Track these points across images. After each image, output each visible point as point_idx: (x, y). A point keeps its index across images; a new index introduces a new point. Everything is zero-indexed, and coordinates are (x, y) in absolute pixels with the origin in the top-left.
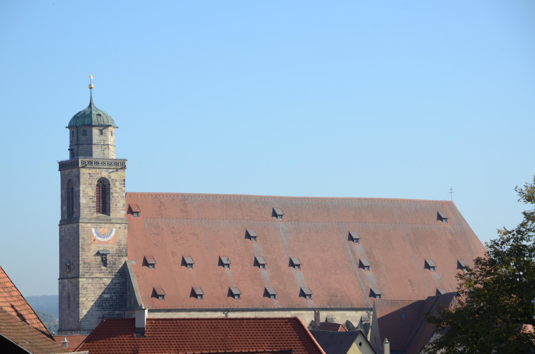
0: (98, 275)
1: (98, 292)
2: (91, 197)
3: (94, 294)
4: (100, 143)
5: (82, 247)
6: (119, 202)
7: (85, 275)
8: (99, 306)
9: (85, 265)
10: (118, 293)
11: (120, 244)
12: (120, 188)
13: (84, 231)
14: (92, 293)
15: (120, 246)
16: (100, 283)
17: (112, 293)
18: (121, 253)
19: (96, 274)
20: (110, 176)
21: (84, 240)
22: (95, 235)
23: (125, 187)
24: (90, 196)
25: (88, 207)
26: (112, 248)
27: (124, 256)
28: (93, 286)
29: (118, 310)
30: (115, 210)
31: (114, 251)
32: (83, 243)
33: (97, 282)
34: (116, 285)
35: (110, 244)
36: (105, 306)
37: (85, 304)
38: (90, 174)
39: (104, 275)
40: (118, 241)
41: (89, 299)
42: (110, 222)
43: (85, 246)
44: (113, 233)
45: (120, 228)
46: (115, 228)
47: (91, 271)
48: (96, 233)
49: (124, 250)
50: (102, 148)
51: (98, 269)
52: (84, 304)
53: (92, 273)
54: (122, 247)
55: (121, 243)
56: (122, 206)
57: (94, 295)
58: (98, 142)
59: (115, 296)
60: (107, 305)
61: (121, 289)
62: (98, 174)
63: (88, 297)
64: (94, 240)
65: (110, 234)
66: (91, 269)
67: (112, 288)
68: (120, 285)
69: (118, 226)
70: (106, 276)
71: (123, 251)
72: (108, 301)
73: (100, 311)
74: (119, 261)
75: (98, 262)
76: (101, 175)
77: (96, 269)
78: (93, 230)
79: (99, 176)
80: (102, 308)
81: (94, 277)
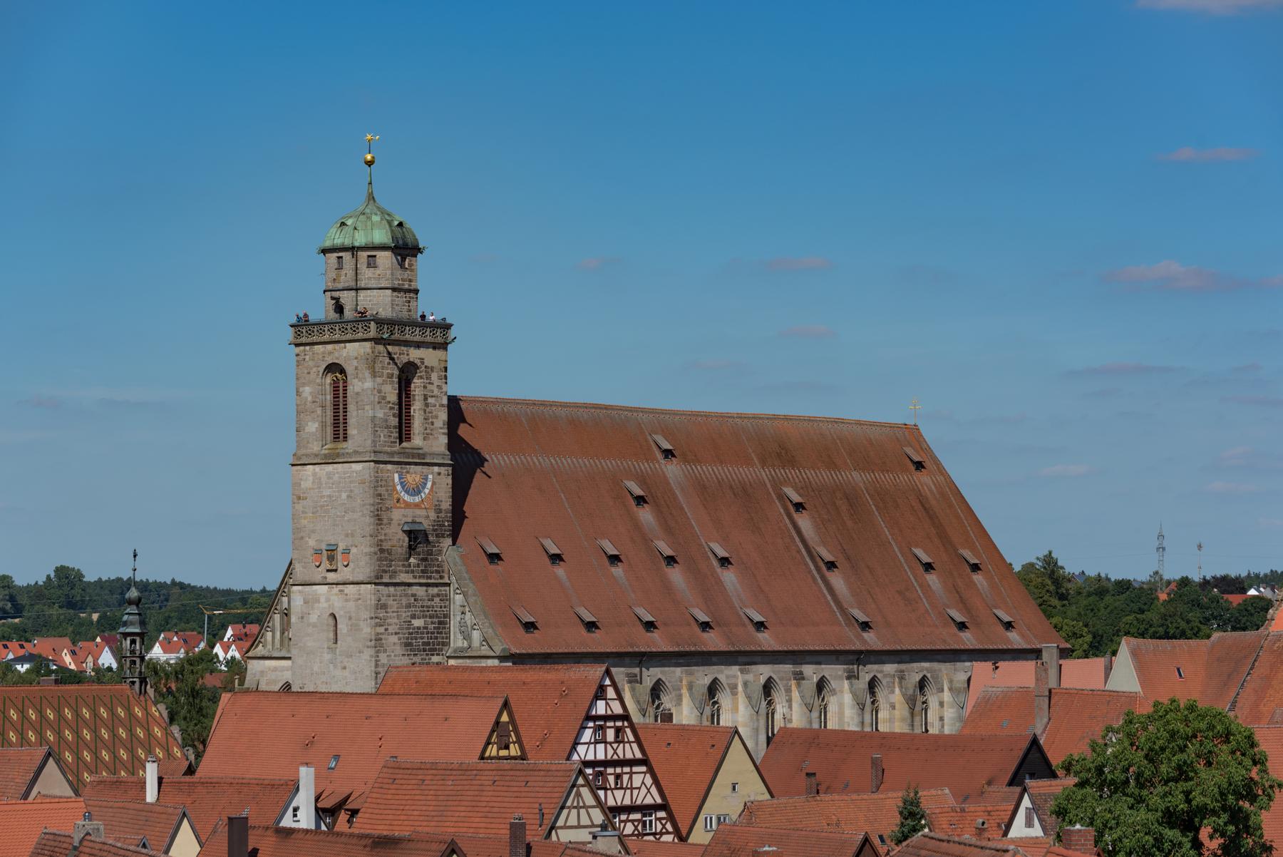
1: (404, 615)
2: (391, 405)
3: (398, 619)
5: (378, 515)
6: (436, 417)
7: (382, 576)
8: (407, 645)
9: (382, 555)
10: (437, 617)
13: (381, 480)
14: (394, 617)
15: (440, 515)
16: (406, 595)
17: (426, 616)
18: (442, 531)
19: (401, 574)
20: (423, 359)
22: (399, 488)
23: (446, 383)
24: (389, 402)
25: (388, 427)
29: (438, 655)
30: (431, 434)
32: (380, 506)
34: (433, 600)
36: (415, 646)
37: (384, 641)
40: (437, 503)
41: (390, 631)
42: (421, 460)
44: (429, 485)
45: (439, 474)
46: (432, 473)
47: (393, 568)
48: (401, 483)
49: (446, 524)
50: (406, 297)
52: (381, 639)
53: (395, 572)
54: (443, 515)
55: (441, 507)
56: (442, 426)
57: (396, 621)
59: (432, 623)
60: (419, 642)
61: (441, 607)
62: (403, 354)
63: (388, 625)
64: (398, 501)
65: (424, 488)
66: (393, 563)
67: (428, 607)
68: (441, 600)
69: (436, 469)
70: (417, 581)
71: (444, 526)
72: (421, 633)
73: (408, 655)
74: (438, 546)
75: (404, 549)
76: (407, 357)
78: (396, 476)
79: (404, 359)
80: (411, 650)
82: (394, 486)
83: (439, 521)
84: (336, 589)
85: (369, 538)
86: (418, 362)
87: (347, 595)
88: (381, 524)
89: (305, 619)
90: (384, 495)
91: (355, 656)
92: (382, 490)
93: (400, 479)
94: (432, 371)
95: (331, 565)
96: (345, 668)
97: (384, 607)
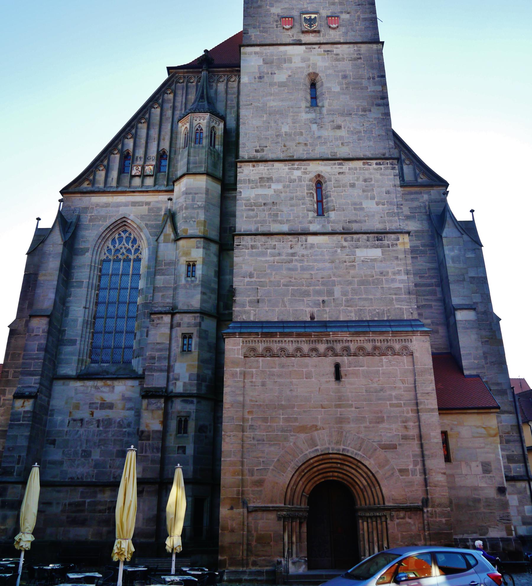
84: (317, 49)
85: (367, 6)
87: (337, 55)
89: (266, 79)
91: (356, 114)
95: (311, 27)
96: (339, 127)
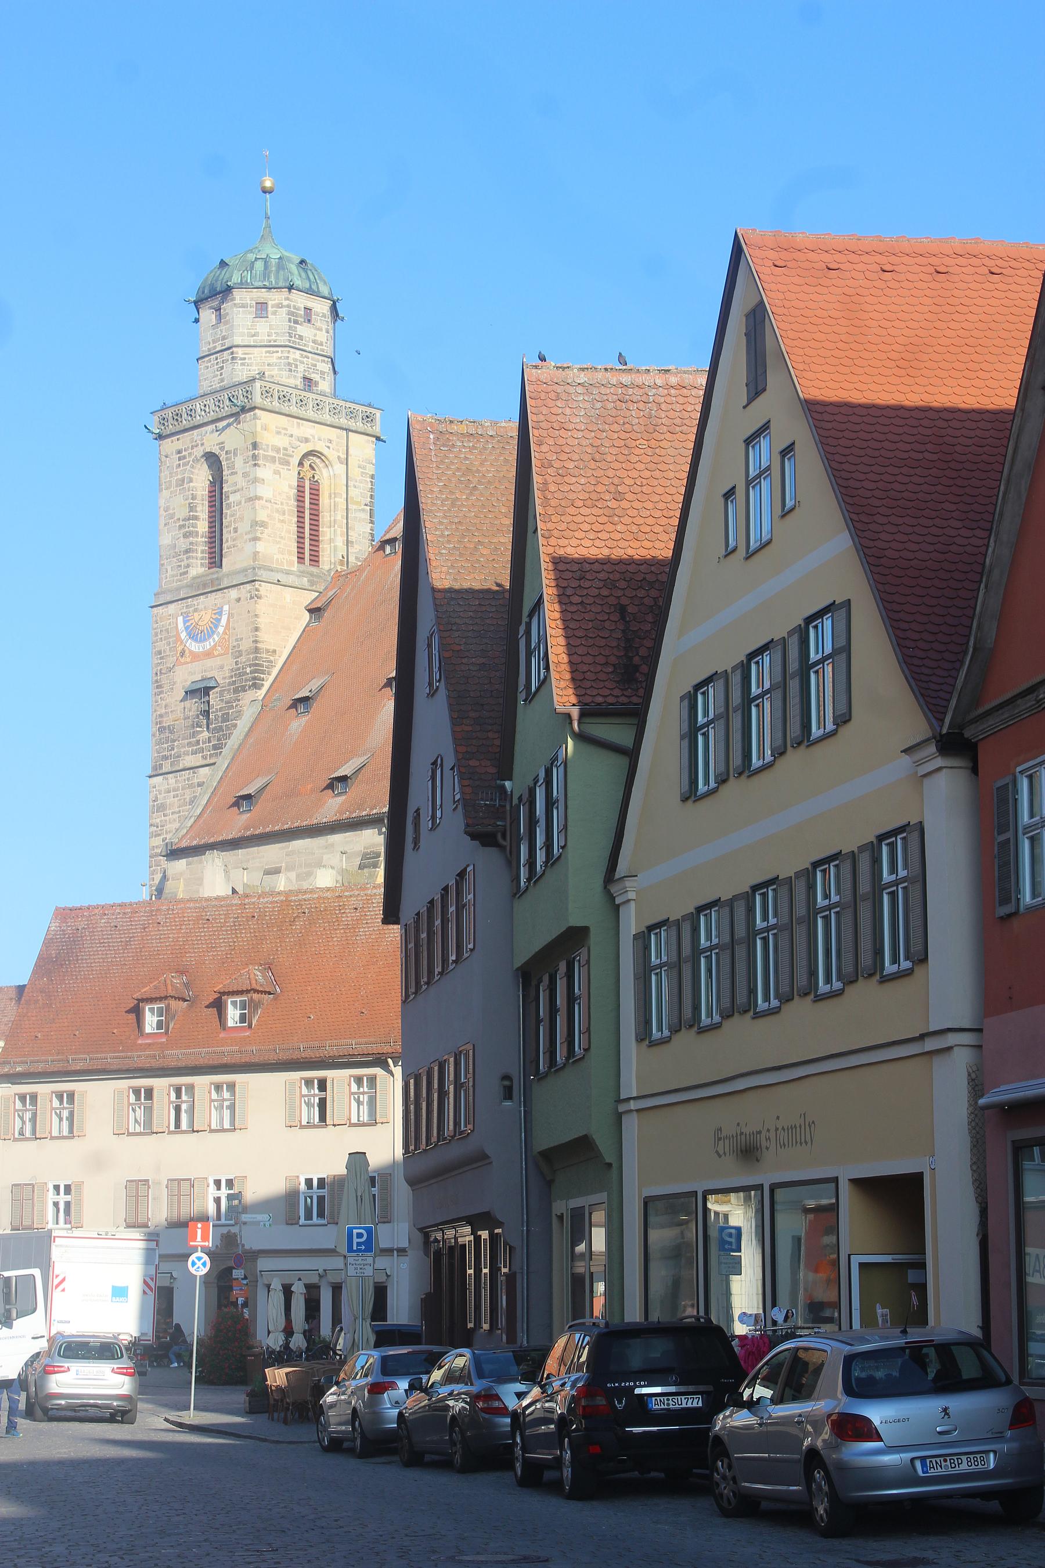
0: (189, 761)
2: (181, 523)
4: (215, 347)
5: (157, 681)
6: (242, 519)
9: (162, 736)
11: (239, 651)
12: (245, 475)
14: (175, 820)
15: (239, 659)
16: (191, 786)
18: (241, 681)
19: (187, 758)
20: (222, 443)
21: (161, 658)
26: (222, 667)
27: (247, 688)
28: (177, 797)
31: (224, 678)
33: (187, 782)
35: (217, 656)
38: (179, 452)
39: (202, 757)
43: (163, 676)
45: (239, 600)
49: (248, 670)
51: (190, 742)
53: (178, 757)
58: (209, 350)
63: (166, 833)
65: (216, 627)
69: (233, 593)
77: (186, 741)
78: (180, 619)
81: (181, 767)
82: (178, 636)
83: (239, 669)
86: (216, 450)
88: (161, 692)
90: (164, 651)
92: (161, 645)
93: (185, 622)
94: (235, 454)
97: (161, 808)
